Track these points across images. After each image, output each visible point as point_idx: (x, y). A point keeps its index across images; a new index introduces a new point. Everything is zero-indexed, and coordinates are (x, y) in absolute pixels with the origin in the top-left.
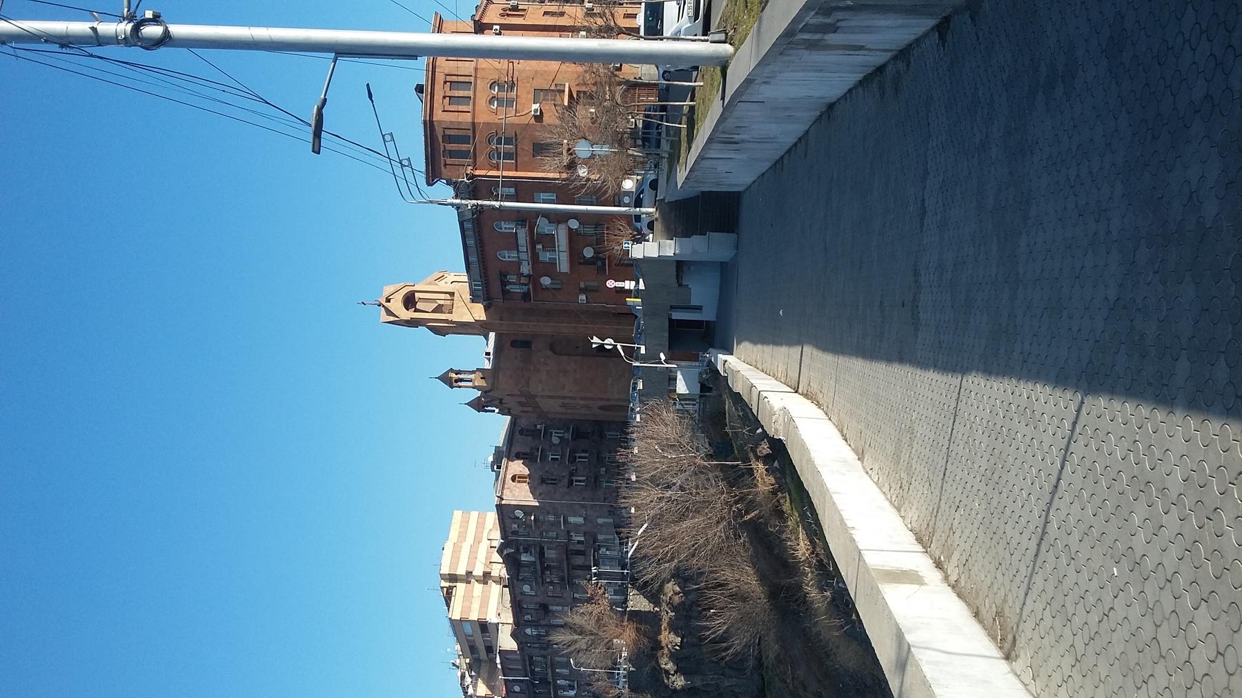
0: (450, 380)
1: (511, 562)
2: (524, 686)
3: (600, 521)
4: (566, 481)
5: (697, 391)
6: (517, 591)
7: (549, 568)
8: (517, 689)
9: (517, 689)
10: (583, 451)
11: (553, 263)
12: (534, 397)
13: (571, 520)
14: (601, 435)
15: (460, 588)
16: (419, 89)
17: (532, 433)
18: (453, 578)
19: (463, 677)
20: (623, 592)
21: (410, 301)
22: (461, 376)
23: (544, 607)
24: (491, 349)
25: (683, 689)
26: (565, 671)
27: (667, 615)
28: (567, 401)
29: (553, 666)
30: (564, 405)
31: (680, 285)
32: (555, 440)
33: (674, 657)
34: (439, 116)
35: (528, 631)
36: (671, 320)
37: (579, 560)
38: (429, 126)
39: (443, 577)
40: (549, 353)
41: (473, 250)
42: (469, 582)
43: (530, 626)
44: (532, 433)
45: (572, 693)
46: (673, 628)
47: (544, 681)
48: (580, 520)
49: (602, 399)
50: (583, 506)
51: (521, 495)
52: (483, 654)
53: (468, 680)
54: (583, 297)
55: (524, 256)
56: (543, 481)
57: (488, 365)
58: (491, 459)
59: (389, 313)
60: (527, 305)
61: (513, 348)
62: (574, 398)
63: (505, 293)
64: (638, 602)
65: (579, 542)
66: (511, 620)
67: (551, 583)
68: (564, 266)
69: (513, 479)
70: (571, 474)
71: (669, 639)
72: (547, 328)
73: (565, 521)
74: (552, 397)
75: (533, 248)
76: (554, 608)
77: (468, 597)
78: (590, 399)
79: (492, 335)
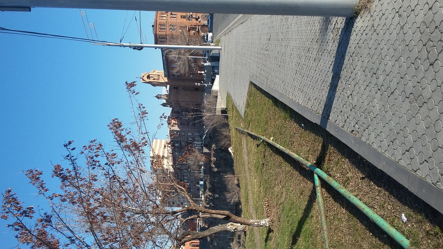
0: (158, 97)
3: (196, 134)
7: (183, 148)
13: (188, 134)
16: (153, 26)
17: (178, 112)
21: (148, 77)
26: (186, 178)
27: (213, 153)
28: (187, 103)
29: (183, 176)
33: (215, 163)
34: (158, 32)
38: (156, 35)
39: (151, 157)
41: (165, 64)
44: (178, 112)
46: (214, 156)
48: (191, 134)
51: (176, 128)
56: (181, 124)
57: (167, 93)
59: (143, 80)
61: (174, 89)
64: (206, 150)
70: (188, 123)
71: (213, 159)
73: (187, 135)
79: (168, 86)
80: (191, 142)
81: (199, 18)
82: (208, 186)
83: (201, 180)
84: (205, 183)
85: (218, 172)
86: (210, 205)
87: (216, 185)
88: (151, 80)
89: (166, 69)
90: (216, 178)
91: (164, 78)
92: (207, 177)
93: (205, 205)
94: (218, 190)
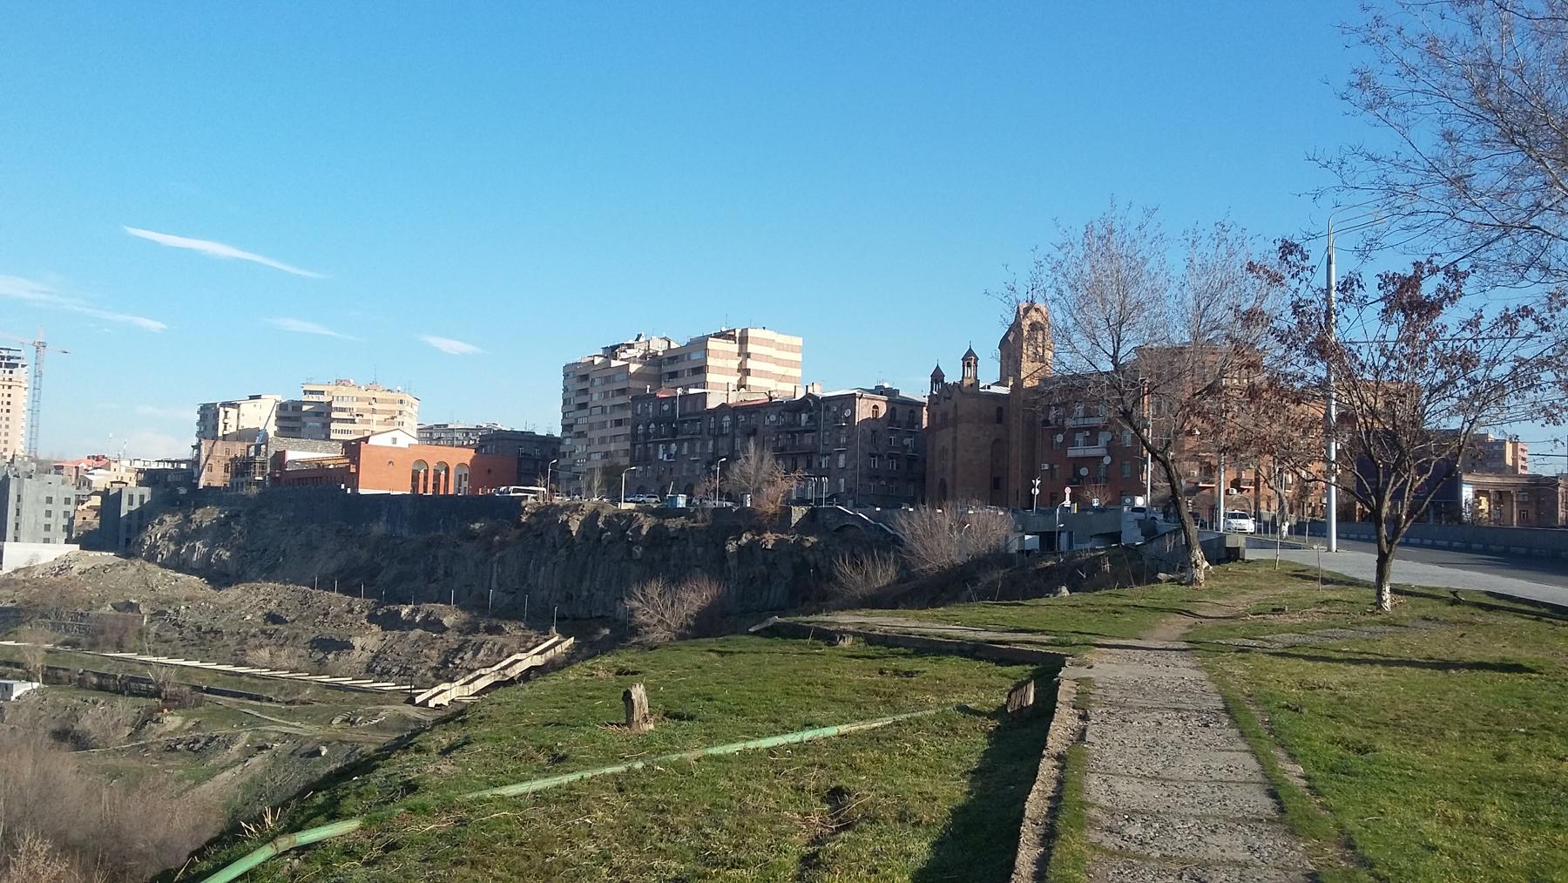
0: (969, 359)
8: (666, 407)
11: (1074, 444)
13: (842, 457)
15: (734, 347)
18: (744, 340)
19: (630, 346)
20: (801, 501)
21: (1034, 326)
26: (685, 451)
29: (691, 441)
30: (944, 449)
32: (907, 441)
35: (727, 418)
37: (802, 463)
46: (778, 542)
47: (675, 432)
48: (841, 464)
51: (863, 411)
52: (668, 369)
55: (1080, 422)
59: (1027, 310)
62: (954, 457)
64: (798, 513)
68: (1071, 453)
71: (770, 539)
74: (955, 439)
77: (726, 355)
80: (815, 464)
81: (1240, 490)
82: (673, 524)
83: (689, 502)
86: (602, 531)
87: (675, 549)
90: (700, 550)
93: (604, 513)
94: (658, 557)
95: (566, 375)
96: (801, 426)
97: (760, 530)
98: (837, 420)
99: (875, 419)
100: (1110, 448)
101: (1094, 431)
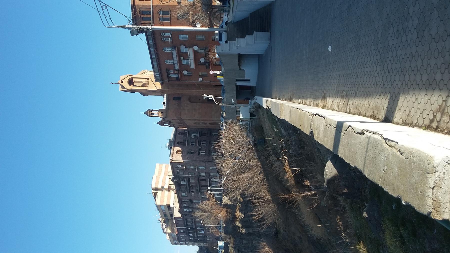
0: (149, 113)
1: (177, 184)
2: (185, 230)
3: (211, 168)
4: (197, 152)
5: (249, 116)
6: (180, 195)
7: (192, 186)
8: (182, 231)
9: (182, 231)
10: (205, 141)
11: (188, 65)
12: (183, 120)
13: (200, 168)
14: (211, 134)
15: (159, 193)
18: (157, 189)
19: (162, 225)
21: (131, 82)
22: (153, 112)
23: (191, 201)
24: (165, 101)
25: (245, 233)
26: (200, 224)
31: (240, 69)
32: (193, 137)
33: (241, 221)
35: (185, 210)
36: (237, 86)
37: (203, 183)
40: (188, 102)
41: (155, 60)
42: (162, 191)
43: (186, 208)
44: (183, 133)
45: (203, 232)
46: (241, 210)
47: (192, 228)
48: (203, 168)
49: (210, 120)
50: (204, 162)
52: (169, 217)
53: (164, 226)
54: (201, 79)
56: (188, 153)
57: (164, 108)
58: (168, 144)
59: (123, 87)
60: (178, 83)
62: (199, 120)
63: (169, 77)
65: (203, 176)
66: (178, 206)
67: (193, 192)
68: (192, 66)
69: (177, 152)
70: (199, 150)
71: (239, 214)
72: (187, 92)
74: (190, 120)
75: (180, 59)
76: (195, 201)
77: (163, 196)
78: (206, 120)
79: (165, 95)
80: (203, 178)
84: (226, 245)
85: (248, 234)
87: (243, 250)
88: (139, 86)
89: (156, 67)
91: (155, 83)
92: (230, 238)
95: (176, 244)
96: (187, 182)
97: (235, 218)
98: (182, 170)
99: (182, 152)
100: (190, 46)
101: (180, 54)
